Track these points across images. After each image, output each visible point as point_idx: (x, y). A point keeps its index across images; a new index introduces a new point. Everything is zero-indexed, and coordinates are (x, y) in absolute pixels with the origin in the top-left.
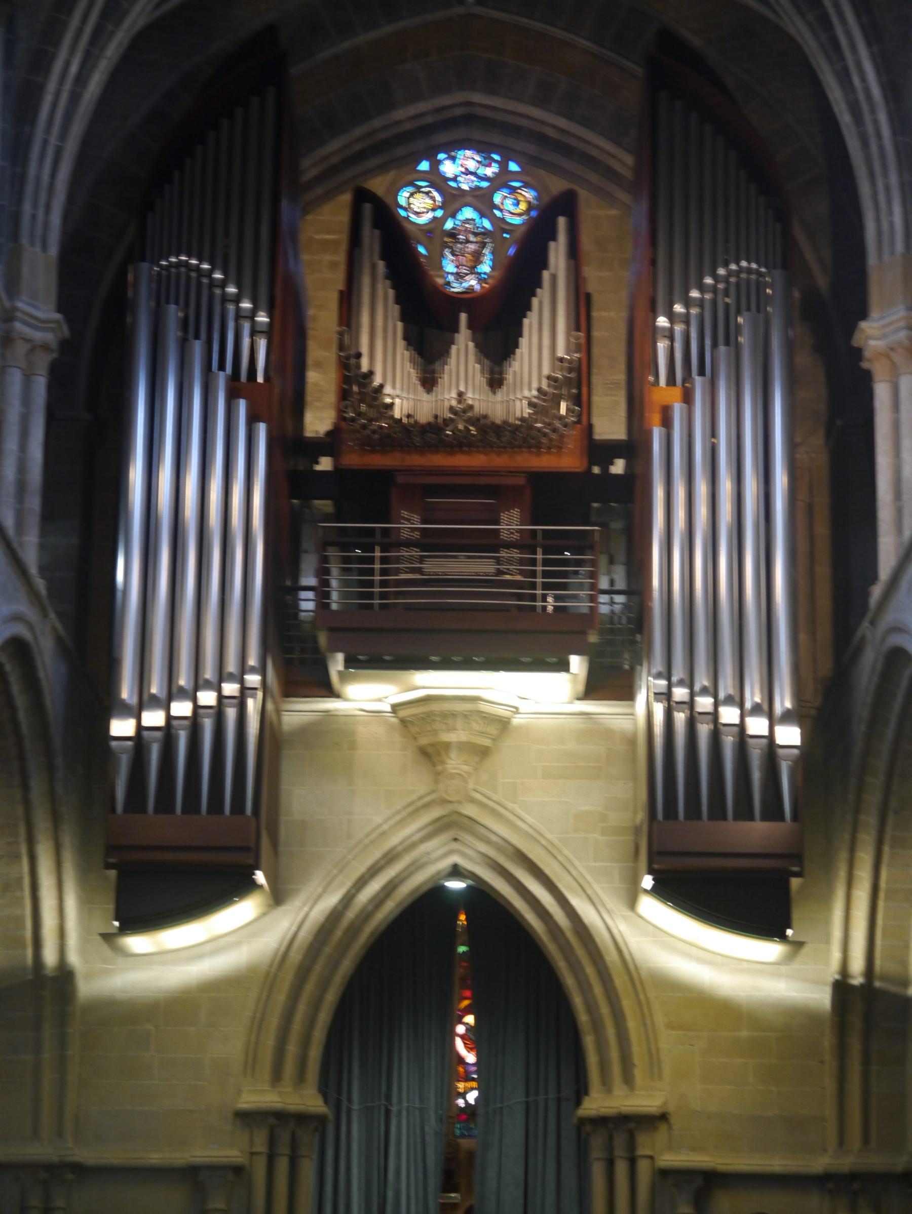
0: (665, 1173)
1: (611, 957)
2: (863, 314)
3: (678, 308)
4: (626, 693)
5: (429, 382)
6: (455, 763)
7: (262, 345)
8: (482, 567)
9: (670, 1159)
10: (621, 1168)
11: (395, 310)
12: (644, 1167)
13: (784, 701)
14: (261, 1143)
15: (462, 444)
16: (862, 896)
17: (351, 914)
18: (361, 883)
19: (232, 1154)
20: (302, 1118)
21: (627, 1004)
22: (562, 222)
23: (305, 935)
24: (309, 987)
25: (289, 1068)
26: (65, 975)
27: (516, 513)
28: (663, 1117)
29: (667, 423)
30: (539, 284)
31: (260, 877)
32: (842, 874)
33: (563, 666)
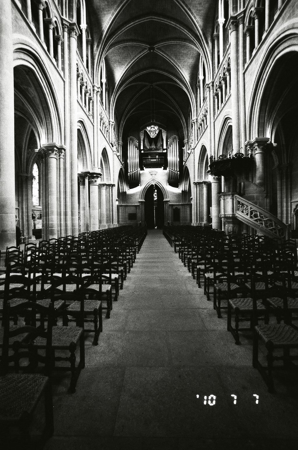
0: (170, 205)
3: (170, 139)
4: (166, 169)
5: (151, 145)
6: (153, 175)
7: (138, 143)
8: (155, 160)
9: (170, 204)
13: (178, 170)
14: (140, 203)
18: (147, 185)
23: (143, 189)
25: (142, 199)
26: (126, 192)
29: (169, 149)
31: (140, 185)
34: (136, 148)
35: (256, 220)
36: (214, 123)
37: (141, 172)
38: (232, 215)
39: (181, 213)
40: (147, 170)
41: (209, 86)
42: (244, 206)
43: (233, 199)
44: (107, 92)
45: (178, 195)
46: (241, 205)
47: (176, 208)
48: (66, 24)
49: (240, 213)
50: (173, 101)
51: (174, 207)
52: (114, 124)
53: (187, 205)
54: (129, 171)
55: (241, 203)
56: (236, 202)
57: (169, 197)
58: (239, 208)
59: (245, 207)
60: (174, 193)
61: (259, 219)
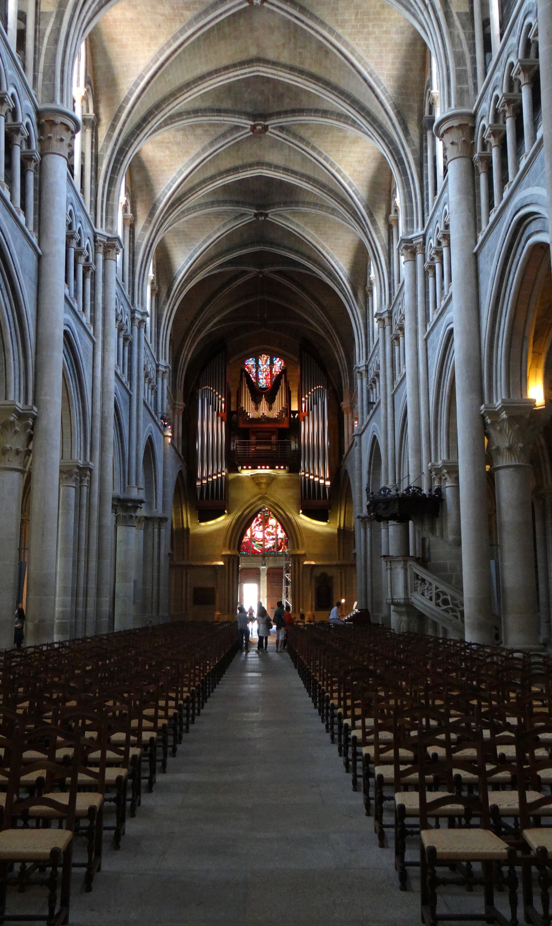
1: (295, 524)
2: (342, 401)
3: (307, 396)
6: (263, 486)
8: (269, 448)
9: (306, 563)
10: (297, 564)
11: (249, 394)
12: (301, 565)
15: (263, 423)
16: (343, 512)
17: (243, 516)
20: (234, 556)
21: (298, 533)
22: (283, 375)
24: (235, 531)
25: (232, 546)
26: (188, 529)
28: (305, 555)
29: (304, 421)
30: (279, 388)
31: (226, 511)
32: (339, 508)
34: (218, 416)
35: (446, 611)
36: (393, 396)
37: (232, 476)
38: (404, 599)
41: (383, 317)
42: (425, 584)
43: (406, 570)
44: (154, 298)
45: (326, 538)
47: (324, 575)
48: (102, 239)
49: (419, 597)
50: (315, 306)
51: (318, 573)
52: (167, 370)
55: (419, 577)
58: (417, 587)
59: (427, 584)
61: (451, 608)
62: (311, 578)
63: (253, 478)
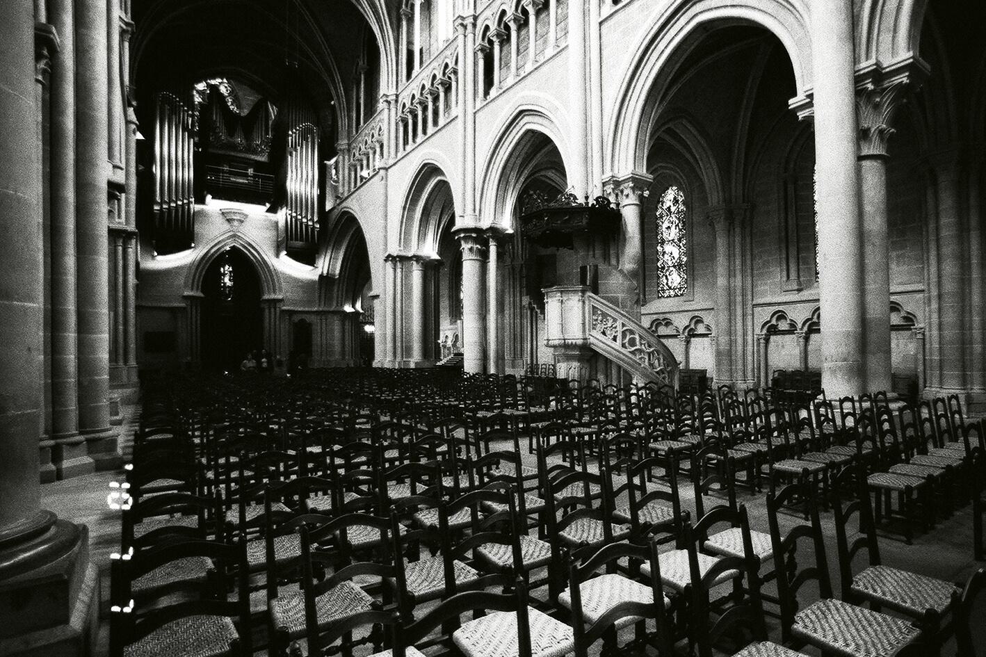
1: (271, 268)
3: (294, 130)
6: (236, 223)
10: (272, 310)
13: (316, 219)
14: (189, 302)
18: (212, 248)
19: (183, 305)
25: (195, 288)
27: (252, 169)
29: (291, 155)
32: (323, 257)
33: (265, 205)
37: (198, 207)
39: (317, 339)
40: (213, 205)
45: (307, 286)
46: (600, 318)
47: (302, 320)
51: (296, 318)
53: (334, 313)
54: (158, 199)
56: (589, 309)
57: (281, 290)
60: (296, 280)
62: (289, 323)
63: (223, 213)
